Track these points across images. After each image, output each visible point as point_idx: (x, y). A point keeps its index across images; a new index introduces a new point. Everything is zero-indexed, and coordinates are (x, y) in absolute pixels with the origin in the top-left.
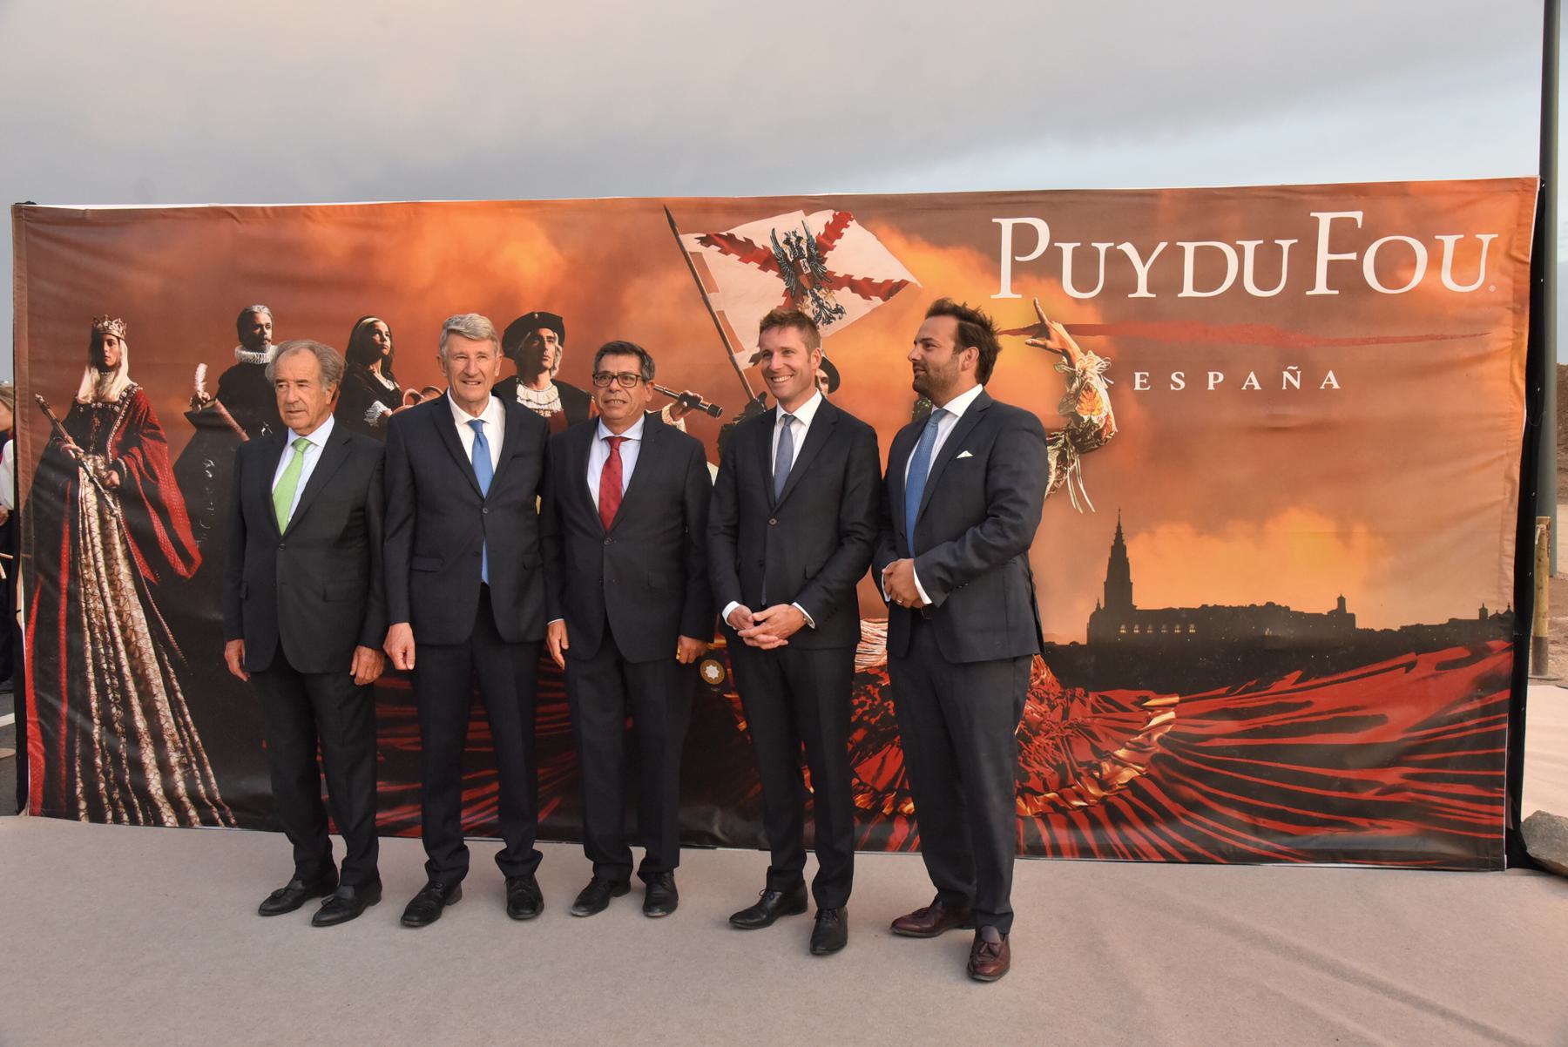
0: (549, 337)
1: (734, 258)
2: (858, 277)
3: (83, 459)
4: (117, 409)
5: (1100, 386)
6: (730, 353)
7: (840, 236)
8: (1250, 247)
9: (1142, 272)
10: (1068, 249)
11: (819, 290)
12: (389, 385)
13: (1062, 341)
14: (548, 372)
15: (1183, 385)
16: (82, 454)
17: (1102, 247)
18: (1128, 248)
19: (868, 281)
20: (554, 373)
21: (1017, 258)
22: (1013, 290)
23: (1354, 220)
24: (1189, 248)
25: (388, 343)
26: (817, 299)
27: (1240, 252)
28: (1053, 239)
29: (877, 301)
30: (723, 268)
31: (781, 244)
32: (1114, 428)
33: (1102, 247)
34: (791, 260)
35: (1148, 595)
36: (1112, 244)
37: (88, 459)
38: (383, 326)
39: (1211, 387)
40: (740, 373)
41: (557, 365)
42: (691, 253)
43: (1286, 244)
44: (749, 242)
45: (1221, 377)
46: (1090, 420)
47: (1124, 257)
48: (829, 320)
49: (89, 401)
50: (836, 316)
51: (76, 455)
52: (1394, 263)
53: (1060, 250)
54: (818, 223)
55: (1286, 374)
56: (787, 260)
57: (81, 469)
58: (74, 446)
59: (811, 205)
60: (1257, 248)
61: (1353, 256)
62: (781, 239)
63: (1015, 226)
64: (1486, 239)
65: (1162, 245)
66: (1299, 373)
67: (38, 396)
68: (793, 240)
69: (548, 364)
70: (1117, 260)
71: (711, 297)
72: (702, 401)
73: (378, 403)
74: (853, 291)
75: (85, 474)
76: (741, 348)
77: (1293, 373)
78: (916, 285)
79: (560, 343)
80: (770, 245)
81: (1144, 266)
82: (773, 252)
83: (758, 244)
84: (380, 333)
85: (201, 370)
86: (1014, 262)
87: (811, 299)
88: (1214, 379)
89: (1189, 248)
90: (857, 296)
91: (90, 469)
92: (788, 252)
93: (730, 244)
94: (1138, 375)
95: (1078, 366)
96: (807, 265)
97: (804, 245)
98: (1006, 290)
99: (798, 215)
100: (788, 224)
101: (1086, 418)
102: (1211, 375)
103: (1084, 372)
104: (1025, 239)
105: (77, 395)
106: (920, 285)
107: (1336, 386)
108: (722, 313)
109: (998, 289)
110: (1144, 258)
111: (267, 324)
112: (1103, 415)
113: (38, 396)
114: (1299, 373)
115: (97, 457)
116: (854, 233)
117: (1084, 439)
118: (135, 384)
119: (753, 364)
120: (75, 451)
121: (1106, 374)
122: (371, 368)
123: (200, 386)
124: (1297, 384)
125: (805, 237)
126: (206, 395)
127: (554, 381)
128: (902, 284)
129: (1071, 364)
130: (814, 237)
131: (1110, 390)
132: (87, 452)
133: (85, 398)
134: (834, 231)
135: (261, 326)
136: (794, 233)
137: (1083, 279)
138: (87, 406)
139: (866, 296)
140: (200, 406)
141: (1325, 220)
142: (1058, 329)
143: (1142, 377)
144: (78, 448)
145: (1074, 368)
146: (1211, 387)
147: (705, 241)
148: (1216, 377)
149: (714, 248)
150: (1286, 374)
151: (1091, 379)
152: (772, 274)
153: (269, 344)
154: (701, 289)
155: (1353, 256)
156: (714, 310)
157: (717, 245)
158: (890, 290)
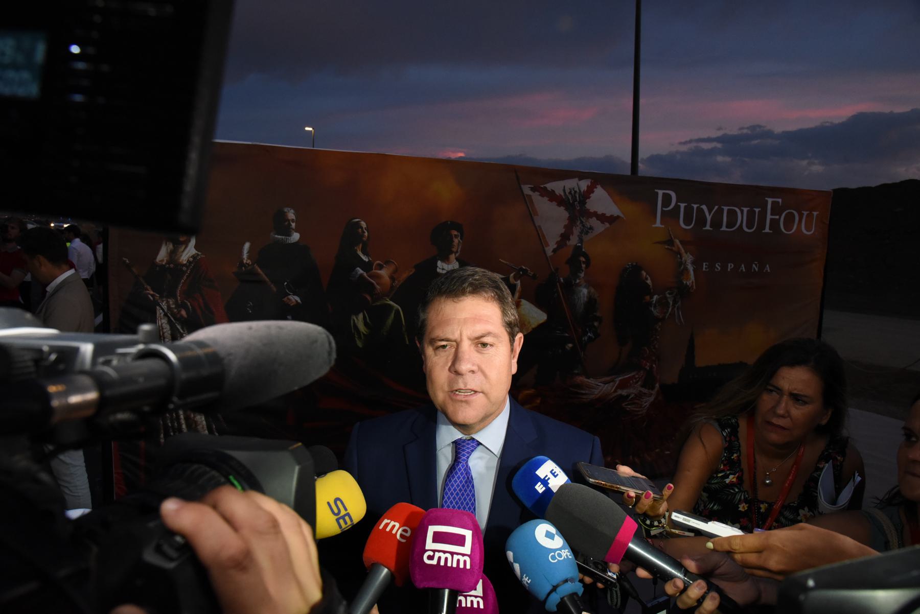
0: (455, 235)
1: (546, 199)
2: (600, 212)
3: (159, 301)
4: (184, 269)
5: (690, 268)
6: (544, 247)
7: (593, 192)
8: (745, 210)
9: (709, 218)
10: (683, 205)
11: (583, 218)
12: (365, 259)
13: (679, 248)
14: (454, 255)
15: (719, 268)
16: (158, 298)
17: (695, 206)
18: (704, 207)
19: (603, 215)
20: (457, 255)
21: (664, 209)
22: (661, 223)
23: (778, 202)
24: (726, 209)
25: (366, 234)
26: (582, 222)
27: (742, 212)
28: (678, 201)
29: (607, 225)
30: (543, 205)
31: (567, 194)
32: (694, 287)
34: (571, 202)
35: (702, 360)
36: (698, 205)
37: (163, 301)
38: (363, 224)
39: (729, 270)
40: (547, 258)
41: (459, 250)
42: (527, 195)
43: (757, 210)
44: (553, 191)
45: (733, 265)
46: (686, 283)
47: (702, 210)
48: (587, 233)
49: (164, 263)
50: (590, 231)
51: (154, 298)
52: (789, 220)
53: (680, 206)
54: (584, 185)
55: (754, 266)
56: (570, 202)
57: (158, 307)
58: (152, 292)
59: (582, 176)
61: (777, 217)
62: (567, 191)
63: (664, 193)
64: (815, 213)
65: (716, 207)
66: (758, 265)
67: (125, 259)
68: (573, 192)
69: (454, 250)
70: (700, 211)
71: (535, 218)
72: (529, 272)
73: (358, 268)
74: (597, 219)
75: (161, 311)
76: (548, 245)
77: (756, 265)
78: (623, 218)
79: (461, 239)
80: (562, 194)
81: (710, 215)
82: (564, 197)
83: (557, 193)
84: (362, 228)
85: (247, 246)
86: (662, 211)
87: (579, 222)
88: (730, 266)
89: (726, 209)
90: (599, 222)
91: (165, 307)
92: (570, 198)
93: (545, 193)
94: (704, 264)
95: (683, 259)
96: (578, 205)
97: (578, 196)
98: (658, 224)
99: (576, 180)
100: (570, 184)
101: (685, 282)
103: (685, 262)
104: (667, 200)
105: (155, 258)
106: (625, 218)
107: (769, 271)
108: (539, 226)
109: (655, 223)
110: (710, 212)
111: (293, 221)
112: (691, 281)
113: (125, 259)
114: (758, 265)
115: (169, 300)
116: (599, 192)
117: (682, 292)
118: (200, 253)
119: (553, 253)
120: (152, 295)
121: (693, 263)
122: (356, 248)
123: (245, 256)
124: (757, 269)
125: (578, 191)
126: (249, 261)
127: (457, 259)
128: (618, 217)
129: (681, 258)
130: (582, 191)
131: (694, 271)
132: (161, 297)
133: (162, 261)
134: (590, 190)
135: (289, 220)
136: (574, 189)
137: (688, 221)
138: (162, 266)
139: (603, 222)
140: (243, 268)
141: (770, 200)
142: (677, 241)
143: (706, 265)
144: (155, 293)
145: (682, 259)
146: (729, 270)
147: (533, 189)
148: (731, 266)
149: (537, 193)
150: (754, 266)
151: (688, 265)
152: (562, 208)
153: (293, 231)
154: (531, 214)
155: (777, 217)
156: (537, 225)
157: (538, 191)
158: (612, 220)
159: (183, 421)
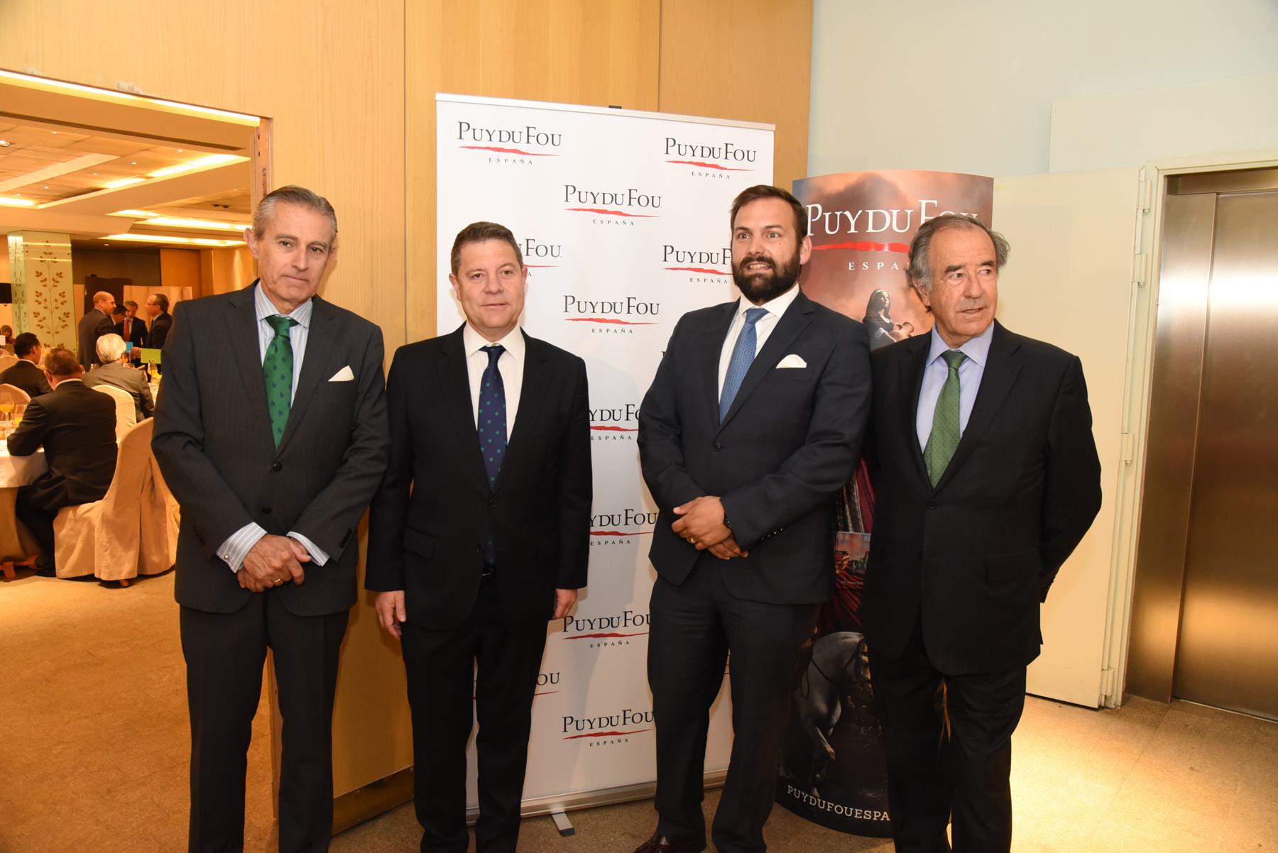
8: (895, 212)
10: (827, 215)
15: (867, 267)
17: (838, 213)
18: (847, 213)
28: (823, 211)
33: (838, 213)
39: (878, 268)
45: (883, 265)
60: (898, 213)
65: (860, 212)
70: (844, 218)
81: (854, 219)
94: (850, 264)
102: (879, 263)
137: (832, 228)
159: (845, 495)
